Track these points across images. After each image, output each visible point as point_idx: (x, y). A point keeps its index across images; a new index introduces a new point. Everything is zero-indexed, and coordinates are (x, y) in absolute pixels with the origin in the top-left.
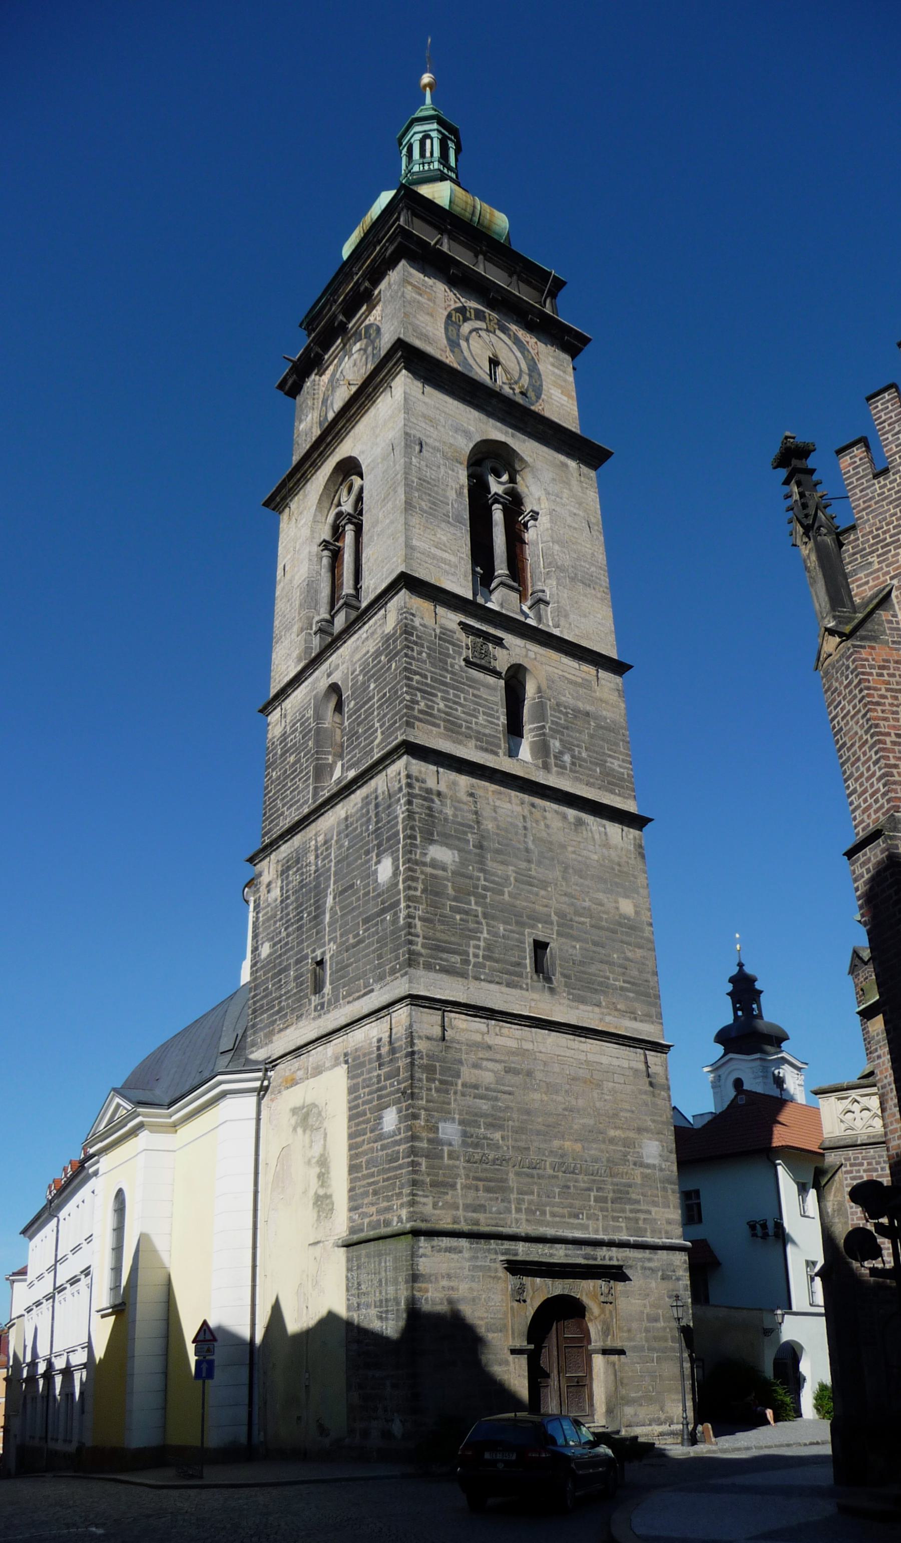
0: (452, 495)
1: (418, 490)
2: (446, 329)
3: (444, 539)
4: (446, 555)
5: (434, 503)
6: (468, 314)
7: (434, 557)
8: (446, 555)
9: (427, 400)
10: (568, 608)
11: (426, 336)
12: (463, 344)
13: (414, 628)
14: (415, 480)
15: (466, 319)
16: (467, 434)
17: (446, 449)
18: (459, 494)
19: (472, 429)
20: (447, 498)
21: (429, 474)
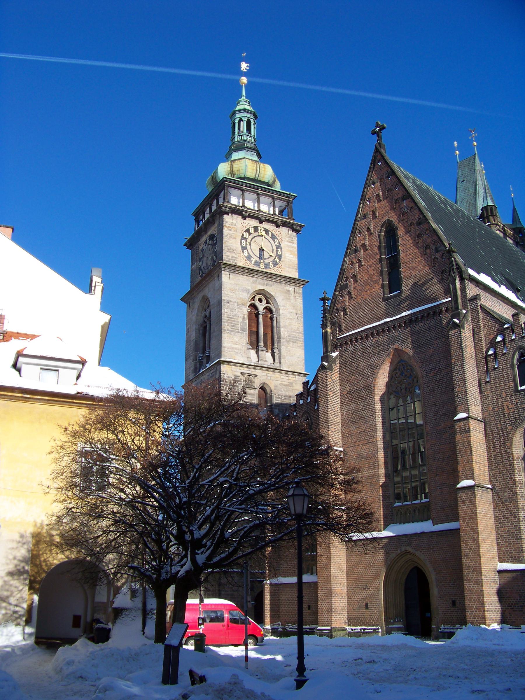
0: (240, 320)
1: (227, 322)
2: (241, 243)
3: (237, 340)
4: (237, 346)
5: (233, 326)
6: (251, 232)
7: (233, 348)
8: (237, 346)
9: (231, 281)
10: (285, 355)
11: (233, 250)
12: (248, 247)
13: (224, 379)
14: (226, 318)
15: (250, 234)
16: (247, 291)
17: (239, 301)
18: (243, 319)
19: (250, 288)
20: (238, 322)
21: (231, 314)
